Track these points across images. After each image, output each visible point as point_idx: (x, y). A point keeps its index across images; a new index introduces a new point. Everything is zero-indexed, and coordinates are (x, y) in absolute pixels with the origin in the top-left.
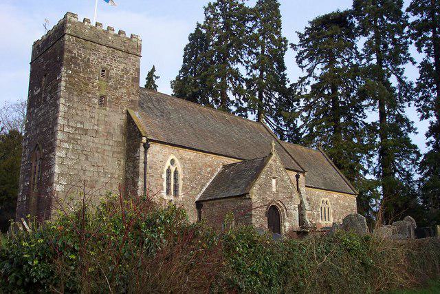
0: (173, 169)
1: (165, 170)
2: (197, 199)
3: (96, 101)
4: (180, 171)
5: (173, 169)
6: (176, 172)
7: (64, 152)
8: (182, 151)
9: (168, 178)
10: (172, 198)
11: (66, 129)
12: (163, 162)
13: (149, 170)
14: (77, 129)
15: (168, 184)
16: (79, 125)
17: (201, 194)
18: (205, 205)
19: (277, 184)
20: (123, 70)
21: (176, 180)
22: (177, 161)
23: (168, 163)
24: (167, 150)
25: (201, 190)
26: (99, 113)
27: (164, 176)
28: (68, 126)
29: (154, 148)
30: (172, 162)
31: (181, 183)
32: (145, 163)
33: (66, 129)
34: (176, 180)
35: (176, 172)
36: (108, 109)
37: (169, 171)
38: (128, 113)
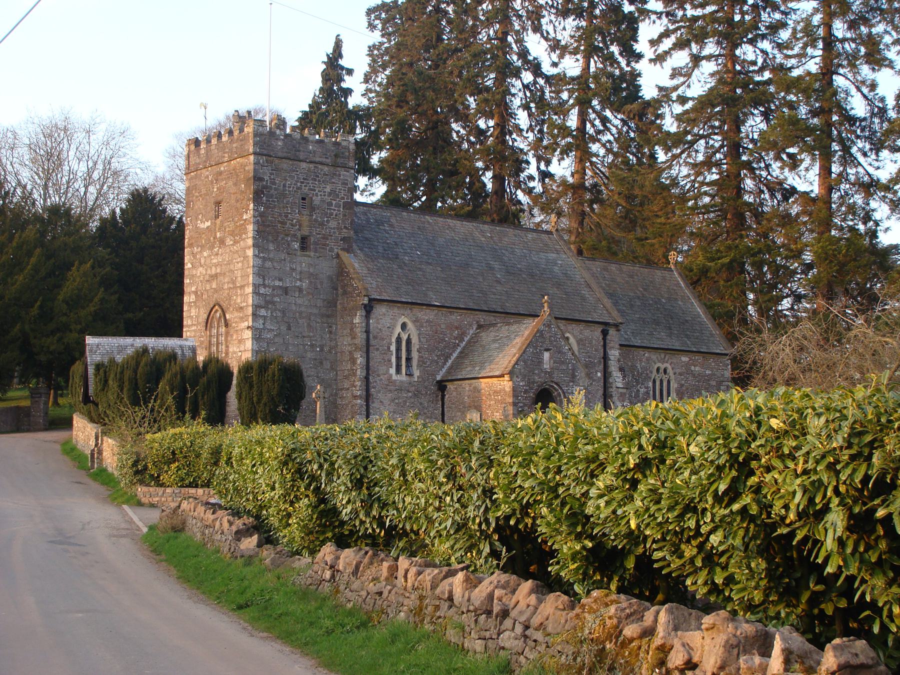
0: (404, 337)
1: (394, 340)
2: (439, 378)
3: (296, 245)
4: (415, 340)
5: (404, 337)
6: (409, 341)
7: (261, 321)
8: (416, 310)
9: (398, 349)
10: (403, 377)
11: (262, 290)
12: (392, 328)
13: (372, 342)
14: (274, 288)
15: (398, 358)
16: (277, 283)
17: (444, 370)
18: (450, 386)
19: (551, 358)
20: (330, 194)
21: (409, 350)
22: (410, 325)
23: (398, 329)
24: (396, 310)
25: (445, 364)
26: (303, 262)
27: (393, 348)
28: (265, 286)
29: (380, 310)
30: (404, 326)
31: (415, 355)
32: (367, 332)
33: (262, 290)
34: (409, 350)
35: (409, 341)
36: (312, 254)
37: (399, 340)
38: (338, 256)
